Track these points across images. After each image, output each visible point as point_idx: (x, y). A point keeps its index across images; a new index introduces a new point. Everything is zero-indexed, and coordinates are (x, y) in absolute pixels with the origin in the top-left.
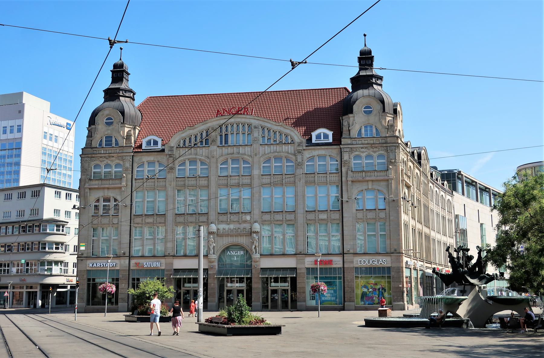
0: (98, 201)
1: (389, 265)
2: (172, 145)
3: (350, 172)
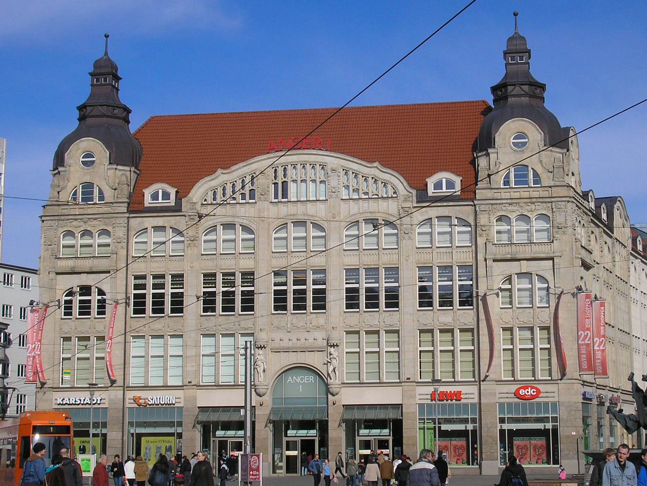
0: (70, 293)
1: (556, 399)
2: (194, 200)
3: (489, 246)
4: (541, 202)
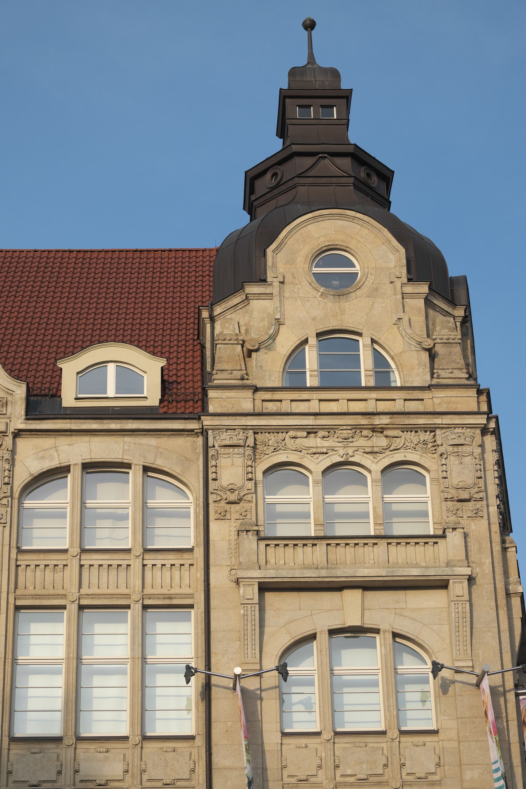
4: (406, 429)
